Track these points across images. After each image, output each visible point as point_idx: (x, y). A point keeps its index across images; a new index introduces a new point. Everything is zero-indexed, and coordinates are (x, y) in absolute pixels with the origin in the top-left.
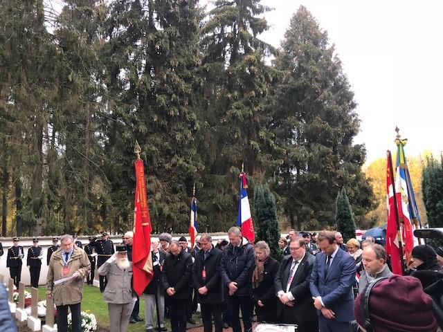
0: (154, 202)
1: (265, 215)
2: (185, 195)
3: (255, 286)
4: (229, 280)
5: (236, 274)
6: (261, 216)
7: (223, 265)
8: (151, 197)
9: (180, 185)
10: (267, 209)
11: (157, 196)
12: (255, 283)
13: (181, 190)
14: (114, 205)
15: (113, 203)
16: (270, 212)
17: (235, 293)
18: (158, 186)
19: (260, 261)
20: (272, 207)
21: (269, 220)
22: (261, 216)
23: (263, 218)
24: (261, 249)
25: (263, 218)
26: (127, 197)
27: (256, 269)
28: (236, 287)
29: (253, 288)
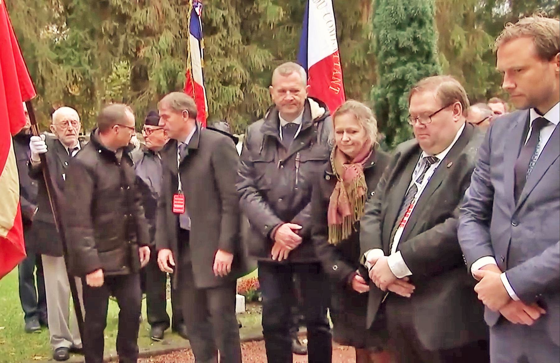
0: (157, 56)
1: (401, 51)
2: (237, 37)
3: (339, 235)
4: (274, 220)
5: (298, 198)
6: (387, 54)
7: (248, 180)
8: (147, 44)
9: (221, 12)
10: (408, 32)
11: (162, 38)
12: (340, 227)
13: (225, 24)
14: (59, 61)
15: (55, 56)
16: (415, 39)
17: (291, 253)
18: (166, 15)
19: (349, 159)
20: (421, 24)
21: (410, 66)
22: (387, 54)
23: (391, 60)
24: (356, 118)
25: (391, 60)
26: (89, 41)
27: (340, 185)
28: (299, 238)
29: (333, 240)
